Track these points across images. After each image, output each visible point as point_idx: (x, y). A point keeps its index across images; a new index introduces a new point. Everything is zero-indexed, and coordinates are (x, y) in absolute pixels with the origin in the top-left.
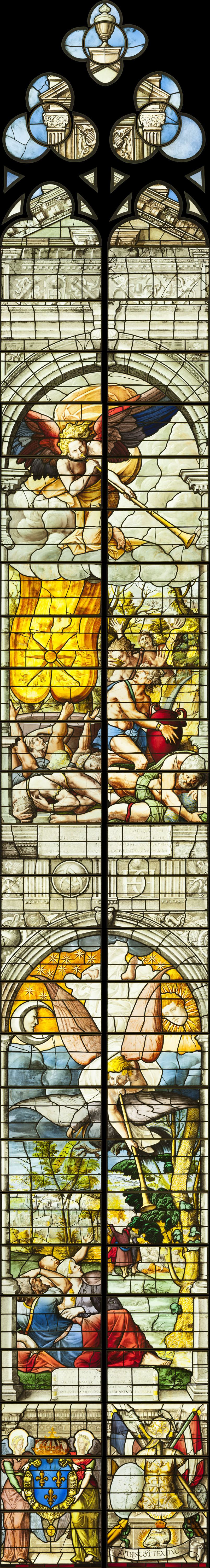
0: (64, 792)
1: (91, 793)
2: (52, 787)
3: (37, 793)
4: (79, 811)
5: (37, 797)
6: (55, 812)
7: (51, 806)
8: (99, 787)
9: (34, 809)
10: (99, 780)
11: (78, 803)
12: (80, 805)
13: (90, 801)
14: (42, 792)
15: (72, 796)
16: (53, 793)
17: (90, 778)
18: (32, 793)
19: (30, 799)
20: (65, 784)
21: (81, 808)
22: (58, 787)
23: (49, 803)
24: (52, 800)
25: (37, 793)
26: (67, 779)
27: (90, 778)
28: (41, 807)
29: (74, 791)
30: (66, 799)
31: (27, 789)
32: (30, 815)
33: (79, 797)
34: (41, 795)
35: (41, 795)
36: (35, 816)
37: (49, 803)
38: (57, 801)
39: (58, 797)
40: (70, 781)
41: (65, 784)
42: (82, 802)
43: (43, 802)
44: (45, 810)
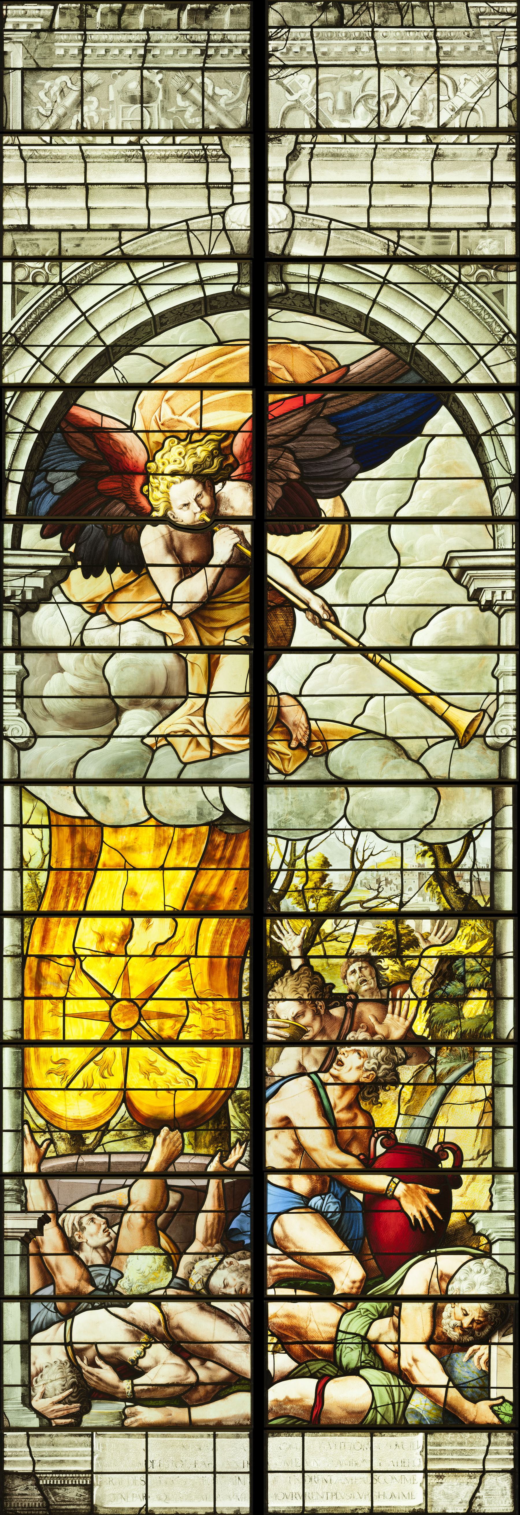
0: (159, 1351)
1: (226, 1353)
2: (127, 1338)
3: (91, 1353)
4: (196, 1396)
6: (136, 1399)
7: (126, 1385)
8: (246, 1337)
9: (85, 1392)
10: (245, 1321)
11: (192, 1378)
13: (223, 1373)
14: (104, 1349)
15: (178, 1360)
16: (130, 1352)
17: (223, 1315)
18: (80, 1353)
19: (75, 1368)
20: (161, 1329)
21: (202, 1390)
22: (144, 1338)
23: (122, 1378)
24: (128, 1370)
25: (91, 1353)
26: (166, 1317)
27: (223, 1315)
28: (102, 1387)
30: (163, 1367)
31: (68, 1344)
32: (75, 1407)
33: (194, 1363)
34: (102, 1357)
35: (102, 1357)
36: (86, 1409)
37: (122, 1378)
38: (142, 1372)
39: (143, 1363)
40: (174, 1322)
41: (161, 1329)
43: (108, 1374)
44: (110, 1395)
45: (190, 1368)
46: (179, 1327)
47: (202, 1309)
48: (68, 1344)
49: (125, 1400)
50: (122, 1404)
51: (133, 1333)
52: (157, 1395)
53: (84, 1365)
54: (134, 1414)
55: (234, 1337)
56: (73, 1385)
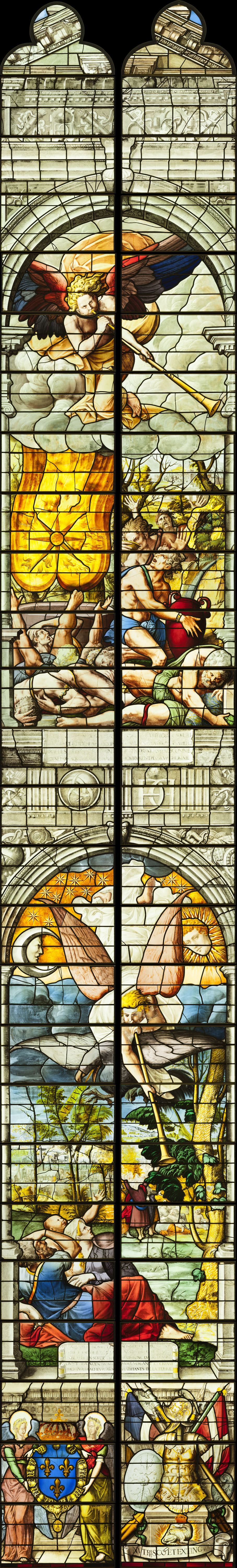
0: (72, 692)
2: (58, 686)
3: (41, 693)
4: (89, 713)
5: (42, 698)
6: (62, 714)
7: (57, 708)
8: (112, 686)
9: (39, 711)
10: (112, 678)
11: (87, 705)
12: (90, 707)
13: (102, 702)
14: (47, 691)
15: (81, 696)
16: (59, 693)
17: (102, 676)
18: (37, 693)
19: (34, 700)
20: (74, 682)
21: (92, 710)
22: (66, 686)
23: (56, 704)
24: (58, 701)
25: (41, 693)
26: (76, 677)
27: (102, 676)
28: (46, 709)
29: (84, 690)
30: (74, 700)
31: (31, 689)
32: (34, 718)
33: (89, 697)
36: (39, 719)
37: (56, 704)
38: (65, 702)
39: (65, 697)
40: (79, 679)
41: (74, 682)
42: (93, 703)
43: (49, 703)
44: (50, 712)
45: (87, 700)
46: (82, 681)
47: (92, 673)
48: (31, 689)
49: (57, 714)
50: (56, 717)
51: (61, 684)
52: (72, 712)
53: (38, 698)
54: (61, 721)
55: (107, 685)
56: (33, 708)
